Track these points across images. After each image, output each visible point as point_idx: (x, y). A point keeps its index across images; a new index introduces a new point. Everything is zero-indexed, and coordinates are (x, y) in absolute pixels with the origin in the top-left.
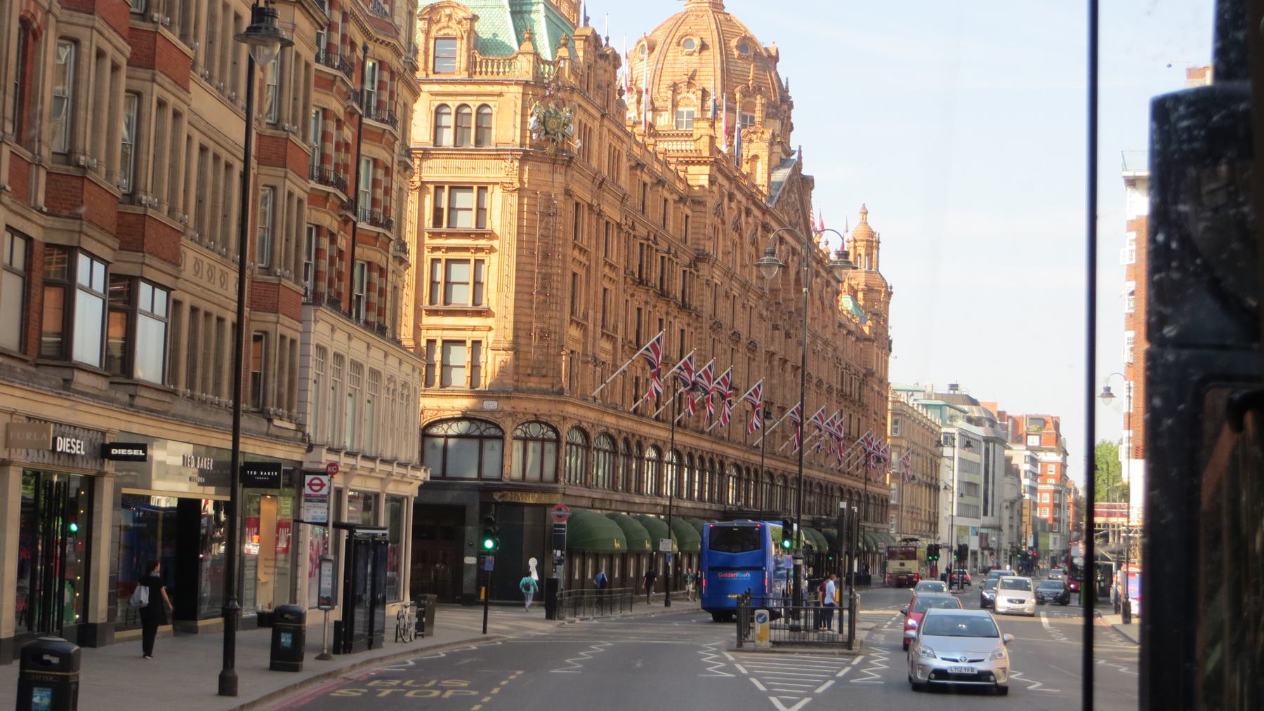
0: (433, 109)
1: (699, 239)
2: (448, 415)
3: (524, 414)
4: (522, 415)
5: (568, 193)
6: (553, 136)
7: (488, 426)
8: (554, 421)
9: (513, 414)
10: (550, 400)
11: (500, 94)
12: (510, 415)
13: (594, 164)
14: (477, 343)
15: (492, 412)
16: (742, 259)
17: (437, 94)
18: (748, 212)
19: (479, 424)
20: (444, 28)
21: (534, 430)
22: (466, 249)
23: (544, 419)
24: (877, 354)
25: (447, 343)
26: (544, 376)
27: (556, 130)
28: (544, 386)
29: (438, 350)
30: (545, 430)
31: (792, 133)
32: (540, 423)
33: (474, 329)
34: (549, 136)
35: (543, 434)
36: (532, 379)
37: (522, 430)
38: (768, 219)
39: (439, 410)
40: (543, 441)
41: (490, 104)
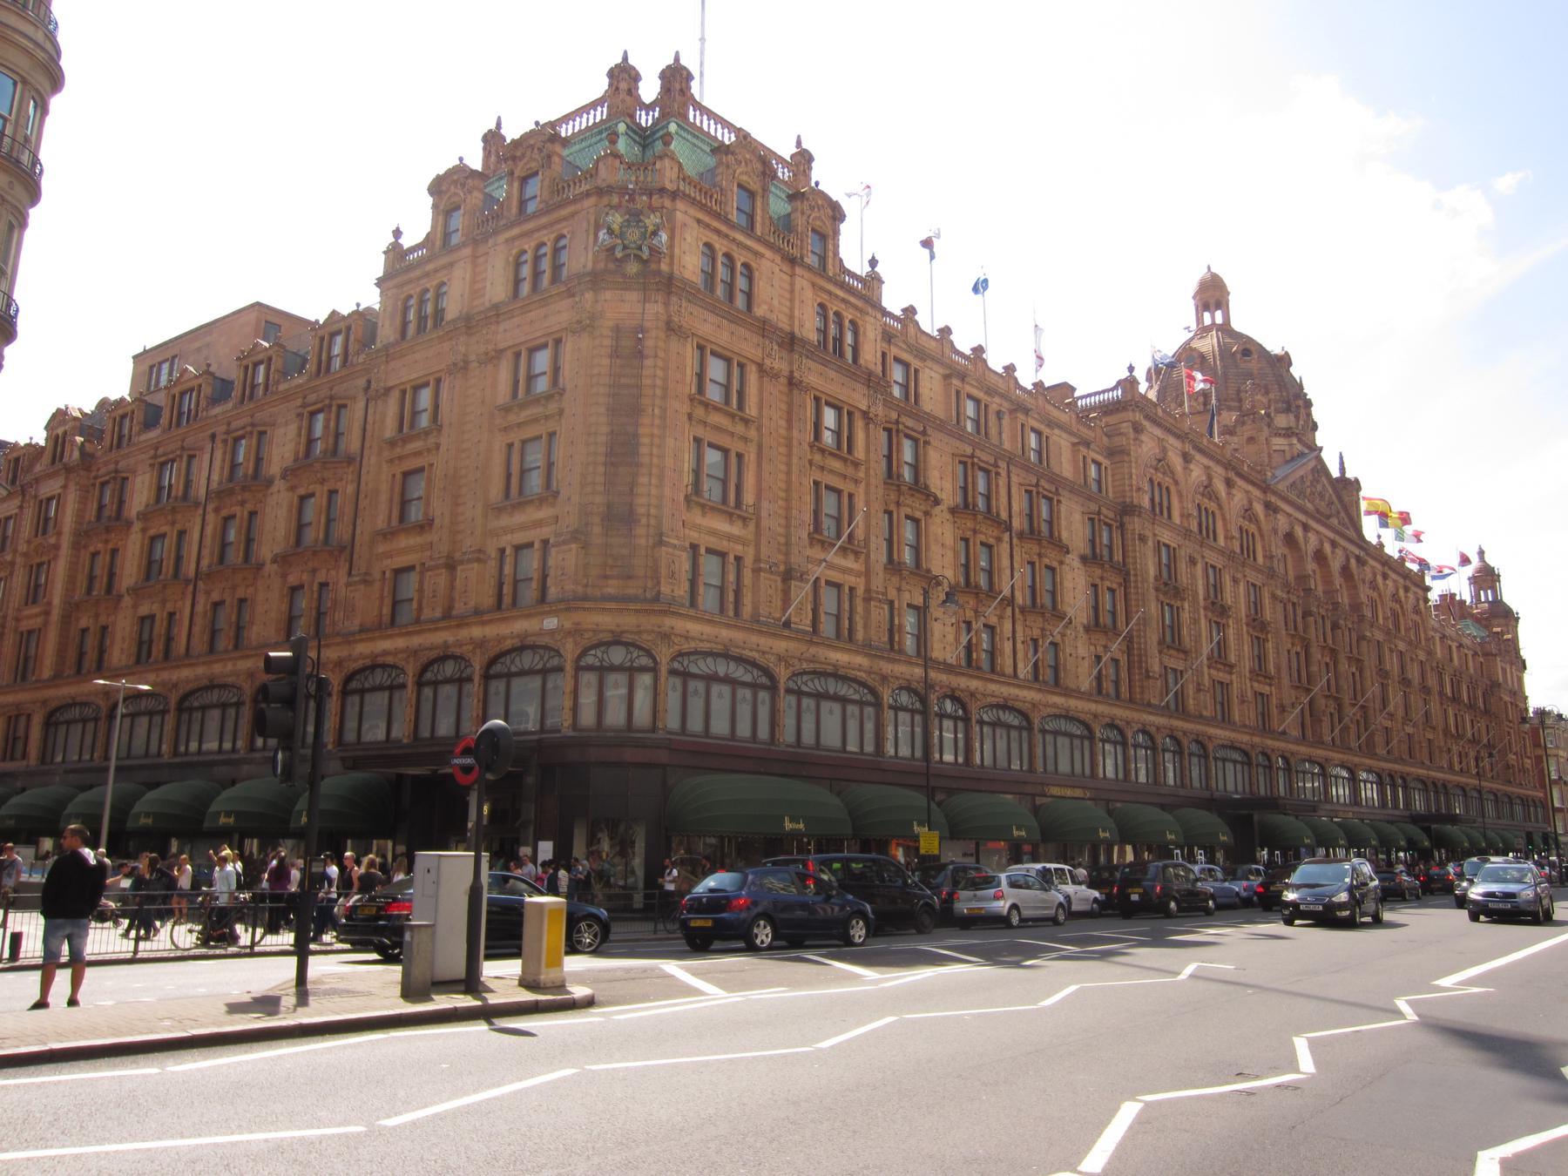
1: (1124, 491)
2: (508, 644)
3: (594, 631)
4: (591, 634)
5: (671, 328)
6: (636, 252)
7: (552, 653)
8: (646, 640)
9: (577, 631)
10: (637, 611)
11: (573, 215)
12: (569, 633)
13: (760, 311)
14: (545, 542)
15: (552, 632)
16: (1226, 530)
17: (514, 239)
18: (1334, 544)
19: (542, 652)
20: (528, 162)
21: (617, 656)
22: (535, 420)
23: (628, 638)
24: (1504, 670)
25: (518, 548)
26: (630, 578)
27: (639, 242)
28: (631, 591)
30: (635, 655)
31: (1317, 434)
32: (626, 644)
33: (539, 524)
34: (628, 251)
35: (632, 661)
38: (1273, 499)
39: (500, 639)
41: (565, 232)
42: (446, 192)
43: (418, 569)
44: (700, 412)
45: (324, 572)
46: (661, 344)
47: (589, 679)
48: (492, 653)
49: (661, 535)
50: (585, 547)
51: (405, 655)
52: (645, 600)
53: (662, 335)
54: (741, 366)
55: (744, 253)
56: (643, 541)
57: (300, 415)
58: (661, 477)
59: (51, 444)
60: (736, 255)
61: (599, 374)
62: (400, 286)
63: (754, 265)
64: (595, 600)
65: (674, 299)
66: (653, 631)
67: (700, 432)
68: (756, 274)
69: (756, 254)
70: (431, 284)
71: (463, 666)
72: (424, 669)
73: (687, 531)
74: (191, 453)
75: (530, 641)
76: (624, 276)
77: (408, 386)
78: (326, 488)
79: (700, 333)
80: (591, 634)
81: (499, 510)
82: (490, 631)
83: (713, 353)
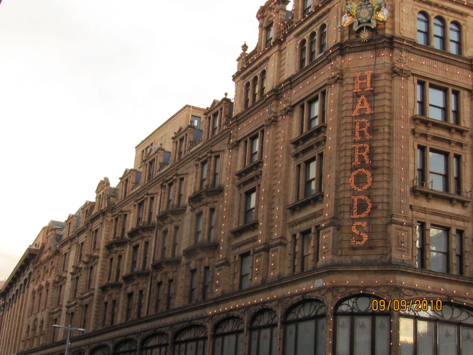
0: (298, 47)
2: (295, 299)
4: (344, 289)
9: (333, 289)
19: (315, 303)
21: (363, 305)
22: (311, 148)
27: (369, 18)
28: (373, 258)
29: (299, 242)
32: (369, 296)
36: (357, 252)
37: (348, 305)
39: (292, 296)
40: (373, 315)
41: (325, 22)
42: (266, 16)
43: (252, 253)
44: (422, 128)
45: (207, 259)
46: (388, 83)
47: (344, 321)
48: (287, 306)
49: (392, 216)
50: (339, 228)
51: (243, 310)
52: (383, 264)
53: (388, 77)
54: (456, 93)
55: (452, 14)
56: (379, 222)
57: (197, 165)
58: (390, 175)
59: (98, 200)
60: (446, 17)
61: (347, 110)
62: (244, 77)
63: (461, 22)
64: (346, 265)
65: (396, 51)
66: (387, 286)
67: (423, 142)
68: (464, 28)
69: (462, 14)
70: (258, 73)
71: (273, 316)
72: (253, 318)
73: (415, 213)
74: (152, 196)
75: (308, 296)
76: (360, 42)
77: (248, 139)
78: (208, 208)
79: (419, 73)
80: (344, 289)
81: (294, 209)
82: (288, 291)
83: (432, 86)
